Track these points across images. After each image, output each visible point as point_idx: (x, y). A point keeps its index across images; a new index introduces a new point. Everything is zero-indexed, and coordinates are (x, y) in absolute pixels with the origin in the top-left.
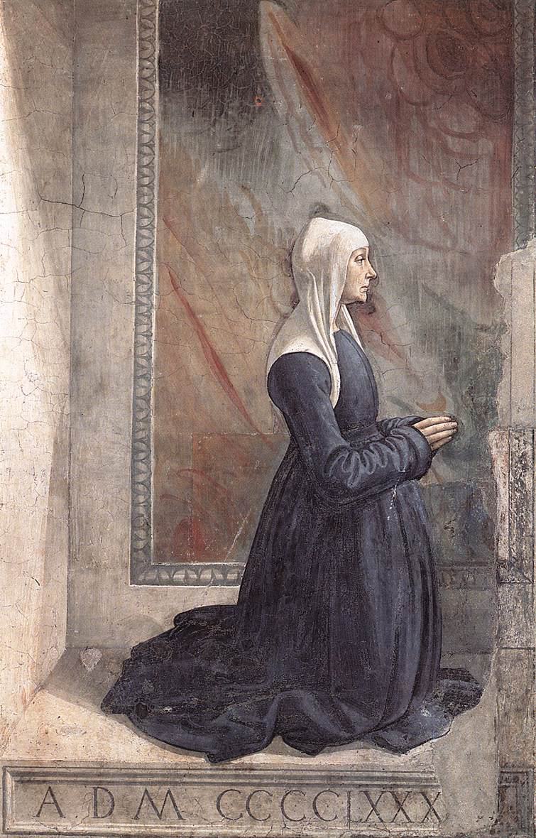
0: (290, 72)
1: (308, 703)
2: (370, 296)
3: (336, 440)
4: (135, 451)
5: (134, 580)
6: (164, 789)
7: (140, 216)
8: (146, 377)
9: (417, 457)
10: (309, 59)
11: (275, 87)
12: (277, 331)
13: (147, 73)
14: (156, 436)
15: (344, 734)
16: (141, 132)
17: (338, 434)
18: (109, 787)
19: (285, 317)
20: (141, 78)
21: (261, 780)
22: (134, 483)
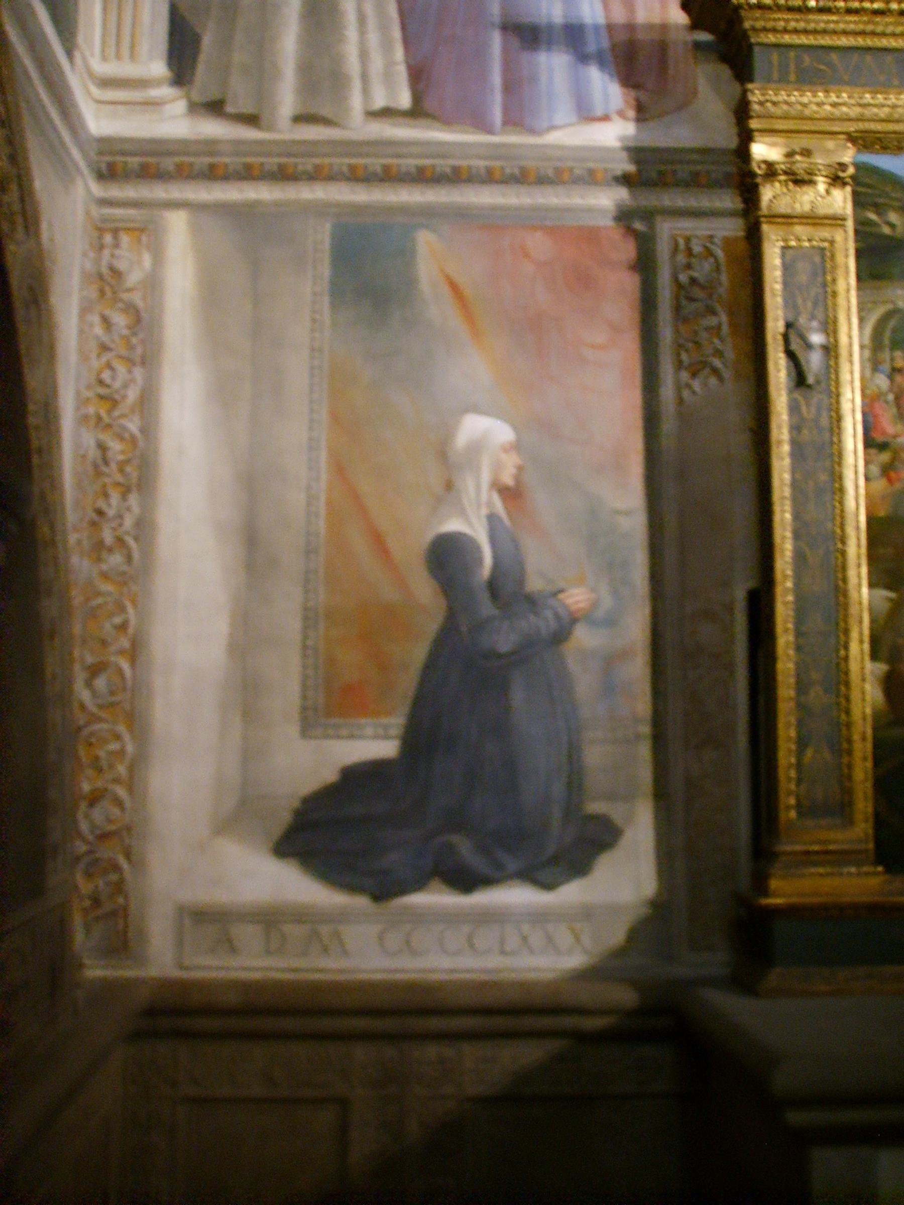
0: (446, 291)
3: (487, 608)
4: (306, 618)
10: (461, 280)
21: (420, 917)
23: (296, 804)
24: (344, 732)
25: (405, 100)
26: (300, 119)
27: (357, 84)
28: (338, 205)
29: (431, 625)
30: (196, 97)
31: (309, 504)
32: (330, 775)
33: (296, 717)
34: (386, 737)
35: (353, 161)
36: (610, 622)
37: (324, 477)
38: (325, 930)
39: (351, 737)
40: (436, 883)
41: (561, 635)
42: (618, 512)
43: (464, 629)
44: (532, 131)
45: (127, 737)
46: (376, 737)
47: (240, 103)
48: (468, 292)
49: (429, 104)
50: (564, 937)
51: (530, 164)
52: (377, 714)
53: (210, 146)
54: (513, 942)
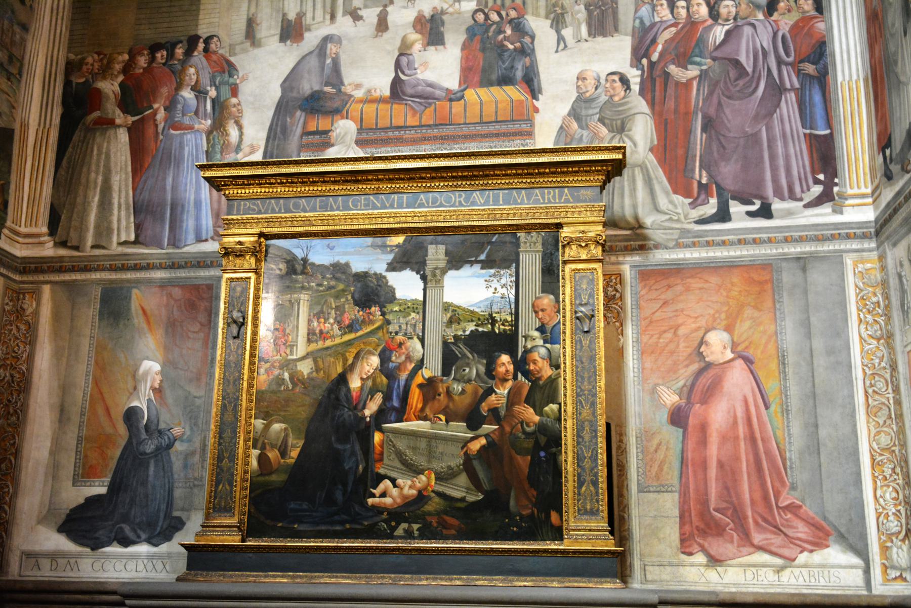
0: (140, 312)
1: (127, 529)
2: (160, 386)
3: (144, 436)
4: (78, 440)
5: (73, 485)
7: (88, 360)
8: (84, 415)
10: (147, 308)
11: (135, 317)
12: (129, 398)
15: (138, 540)
16: (91, 333)
17: (144, 433)
19: (131, 394)
21: (108, 556)
22: (77, 451)
23: (68, 512)
24: (88, 484)
25: (132, 237)
26: (93, 247)
27: (116, 232)
28: (105, 280)
29: (123, 443)
30: (57, 240)
31: (84, 396)
32: (81, 501)
33: (72, 478)
34: (103, 486)
35: (111, 263)
36: (189, 440)
38: (72, 561)
39: (90, 486)
40: (115, 543)
41: (170, 446)
42: (195, 397)
43: (134, 444)
44: (178, 247)
45: (11, 487)
46: (99, 486)
47: (74, 240)
48: (149, 312)
49: (140, 239)
50: (159, 566)
51: (176, 261)
53: (61, 259)
54: (141, 567)
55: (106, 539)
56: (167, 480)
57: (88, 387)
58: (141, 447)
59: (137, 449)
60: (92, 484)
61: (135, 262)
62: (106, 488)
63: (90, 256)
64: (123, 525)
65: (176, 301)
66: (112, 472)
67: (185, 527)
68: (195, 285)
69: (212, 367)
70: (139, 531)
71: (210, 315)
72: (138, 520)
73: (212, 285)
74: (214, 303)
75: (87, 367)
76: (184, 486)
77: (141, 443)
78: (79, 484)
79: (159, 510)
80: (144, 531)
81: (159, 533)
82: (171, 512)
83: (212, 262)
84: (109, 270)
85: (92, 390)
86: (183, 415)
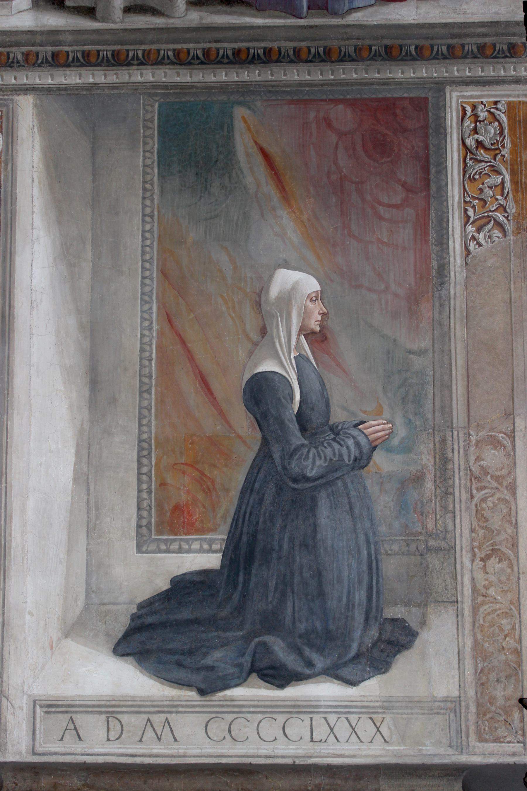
0: (259, 159)
2: (322, 326)
4: (141, 449)
5: (139, 549)
6: (163, 717)
8: (149, 391)
9: (361, 452)
10: (273, 150)
11: (246, 171)
12: (251, 353)
13: (148, 162)
14: (156, 439)
15: (308, 671)
16: (144, 206)
17: (299, 434)
18: (119, 716)
19: (256, 344)
20: (144, 166)
22: (140, 474)
23: (134, 609)
24: (175, 546)
28: (165, 86)
31: (142, 350)
32: (164, 585)
33: (134, 534)
34: (211, 551)
35: (178, 46)
37: (155, 326)
39: (180, 551)
40: (254, 678)
42: (411, 352)
43: (277, 456)
44: (335, 14)
46: (201, 551)
48: (278, 161)
51: (334, 44)
52: (202, 531)
55: (231, 670)
56: (362, 538)
57: (150, 329)
58: (294, 464)
59: (284, 468)
60: (185, 547)
61: (236, 45)
62: (221, 555)
63: (125, 30)
64: (269, 639)
65: (341, 134)
66: (229, 520)
67: (417, 642)
68: (385, 99)
69: (442, 284)
70: (307, 651)
71: (426, 169)
72: (302, 627)
73: (426, 99)
74: (433, 141)
75: (143, 284)
76: (405, 549)
77: (292, 455)
78: (153, 547)
79: (350, 606)
80: (320, 650)
81: (357, 656)
82: (379, 610)
83: (450, 47)
84: (173, 63)
85: (161, 334)
86: (385, 392)
